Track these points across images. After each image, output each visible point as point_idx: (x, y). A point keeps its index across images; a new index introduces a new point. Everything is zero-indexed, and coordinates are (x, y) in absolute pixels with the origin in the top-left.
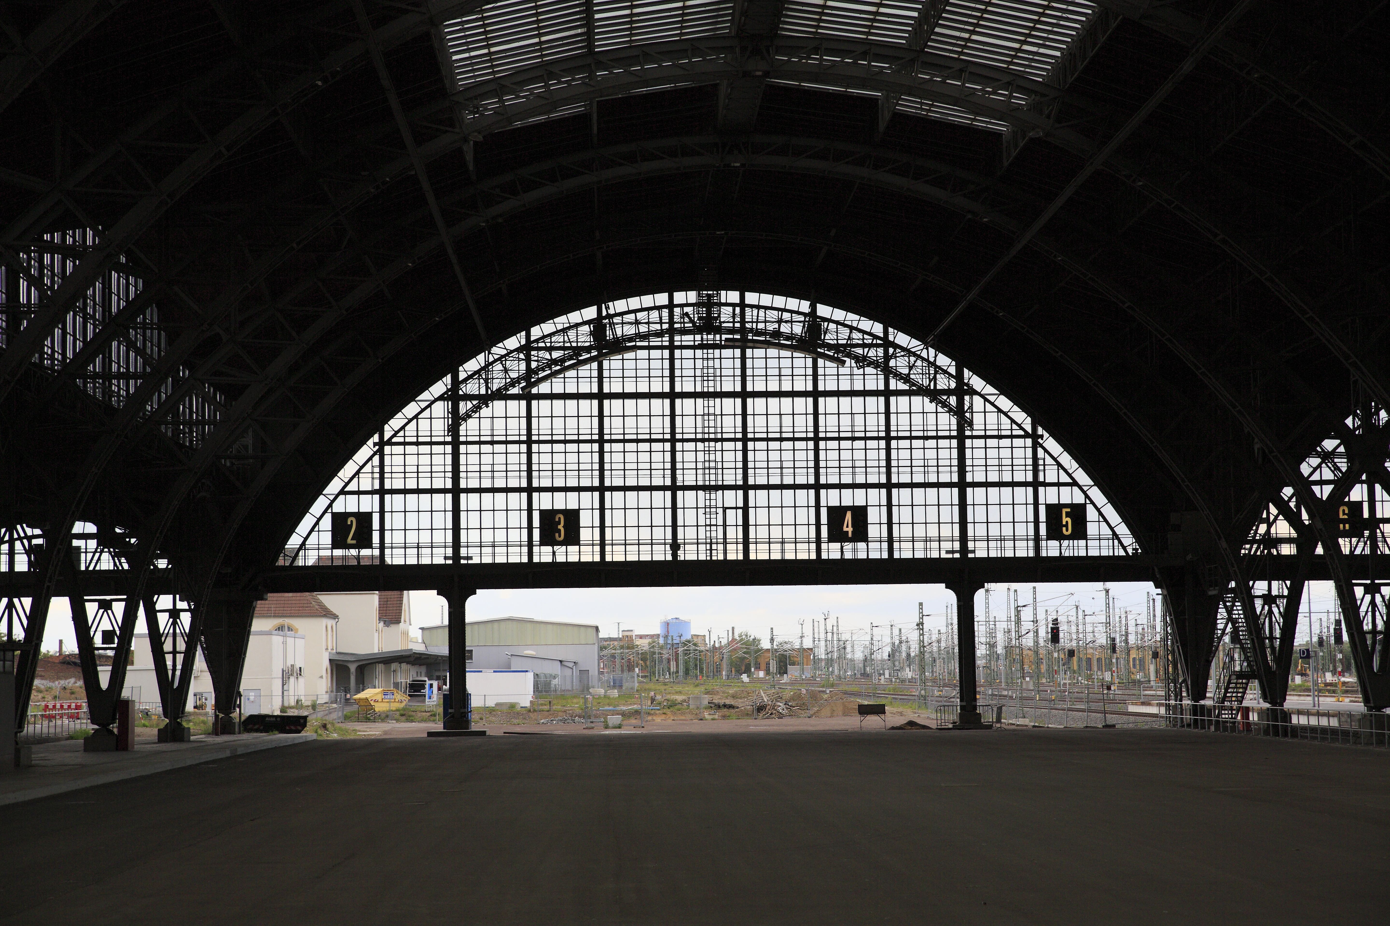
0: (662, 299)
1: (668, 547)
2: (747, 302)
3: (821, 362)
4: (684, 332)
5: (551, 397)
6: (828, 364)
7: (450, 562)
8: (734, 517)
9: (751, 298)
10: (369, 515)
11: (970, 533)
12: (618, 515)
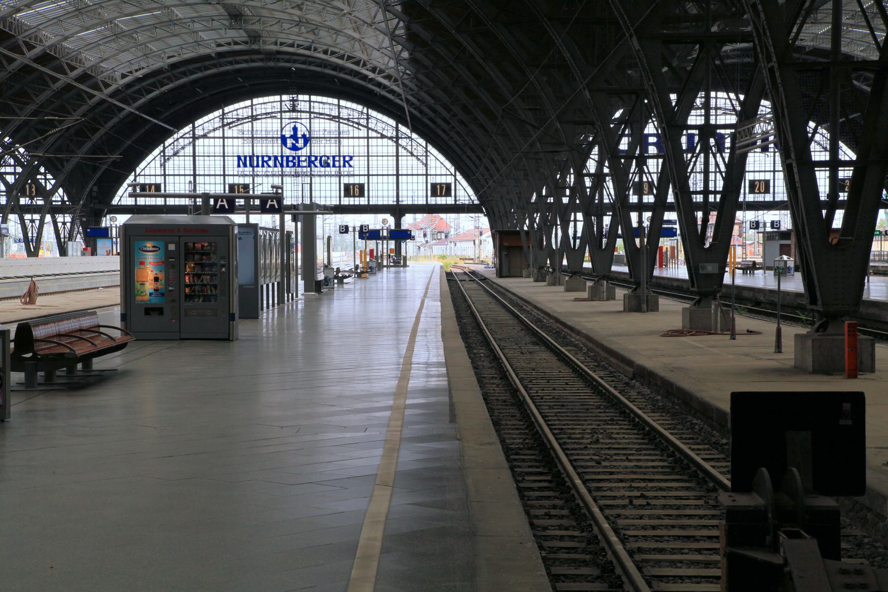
0: (277, 98)
3: (341, 125)
4: (285, 112)
5: (214, 138)
6: (345, 126)
7: (395, 203)
8: (307, 187)
9: (314, 98)
11: (400, 194)
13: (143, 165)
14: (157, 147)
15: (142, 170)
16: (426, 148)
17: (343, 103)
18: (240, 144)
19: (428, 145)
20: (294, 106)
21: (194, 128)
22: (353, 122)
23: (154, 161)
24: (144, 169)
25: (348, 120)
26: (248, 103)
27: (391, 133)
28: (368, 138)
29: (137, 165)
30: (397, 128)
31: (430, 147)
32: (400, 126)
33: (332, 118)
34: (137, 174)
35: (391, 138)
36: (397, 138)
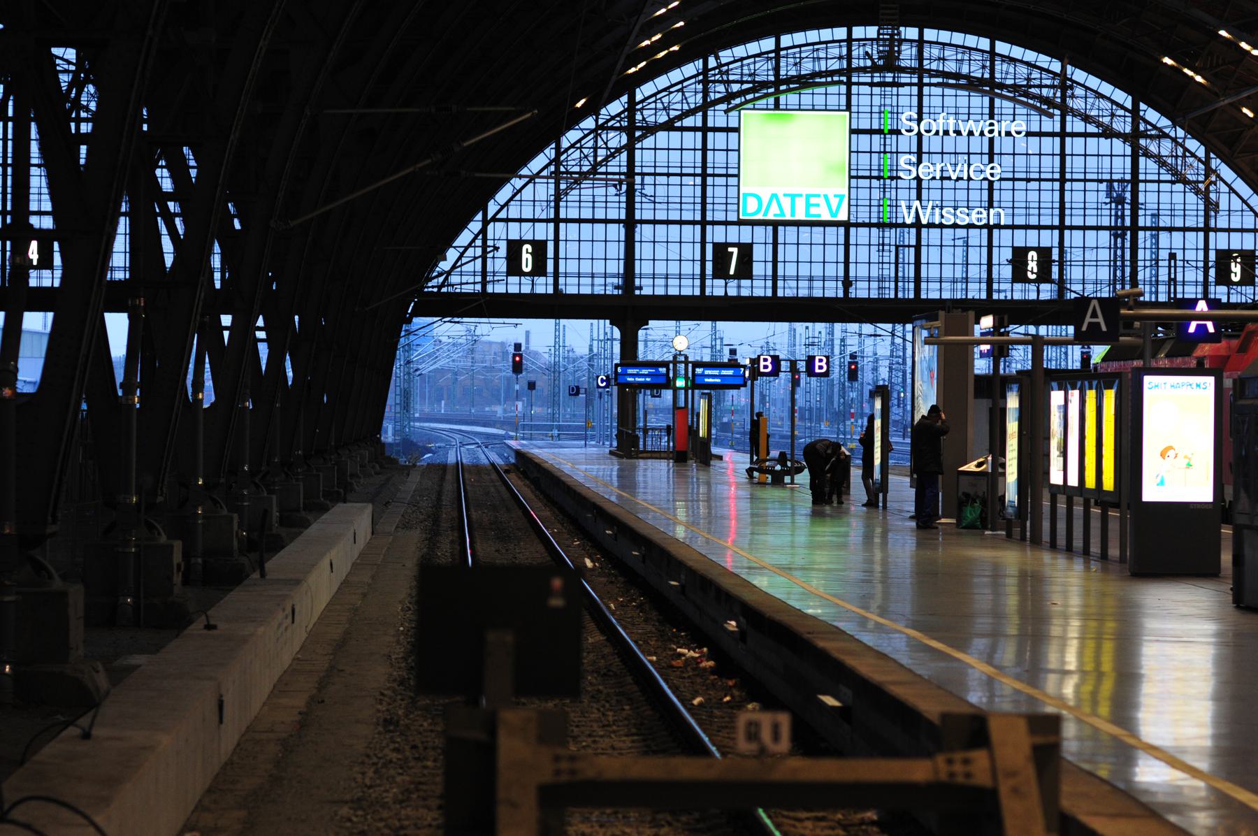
0: (841, 33)
1: (840, 284)
2: (926, 38)
10: (543, 244)
12: (791, 250)
13: (504, 194)
14: (541, 150)
15: (502, 207)
16: (1207, 163)
17: (1002, 47)
18: (876, 148)
19: (1212, 155)
21: (632, 102)
23: (531, 185)
24: (507, 204)
25: (1015, 87)
26: (768, 44)
28: (1063, 134)
29: (491, 194)
30: (1135, 112)
31: (1215, 163)
32: (1143, 106)
33: (973, 85)
34: (489, 216)
35: (1124, 137)
36: (1132, 138)
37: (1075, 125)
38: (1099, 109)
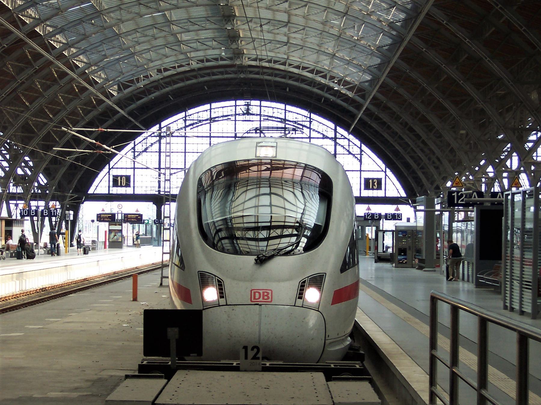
4: (239, 114)
17: (289, 108)
20: (248, 110)
22: (299, 124)
27: (331, 134)
30: (335, 130)
32: (338, 128)
36: (335, 139)
37: (313, 134)
38: (321, 128)
